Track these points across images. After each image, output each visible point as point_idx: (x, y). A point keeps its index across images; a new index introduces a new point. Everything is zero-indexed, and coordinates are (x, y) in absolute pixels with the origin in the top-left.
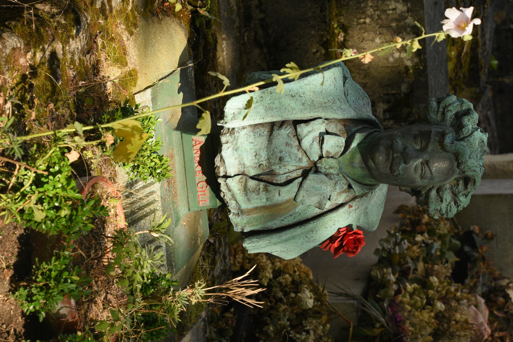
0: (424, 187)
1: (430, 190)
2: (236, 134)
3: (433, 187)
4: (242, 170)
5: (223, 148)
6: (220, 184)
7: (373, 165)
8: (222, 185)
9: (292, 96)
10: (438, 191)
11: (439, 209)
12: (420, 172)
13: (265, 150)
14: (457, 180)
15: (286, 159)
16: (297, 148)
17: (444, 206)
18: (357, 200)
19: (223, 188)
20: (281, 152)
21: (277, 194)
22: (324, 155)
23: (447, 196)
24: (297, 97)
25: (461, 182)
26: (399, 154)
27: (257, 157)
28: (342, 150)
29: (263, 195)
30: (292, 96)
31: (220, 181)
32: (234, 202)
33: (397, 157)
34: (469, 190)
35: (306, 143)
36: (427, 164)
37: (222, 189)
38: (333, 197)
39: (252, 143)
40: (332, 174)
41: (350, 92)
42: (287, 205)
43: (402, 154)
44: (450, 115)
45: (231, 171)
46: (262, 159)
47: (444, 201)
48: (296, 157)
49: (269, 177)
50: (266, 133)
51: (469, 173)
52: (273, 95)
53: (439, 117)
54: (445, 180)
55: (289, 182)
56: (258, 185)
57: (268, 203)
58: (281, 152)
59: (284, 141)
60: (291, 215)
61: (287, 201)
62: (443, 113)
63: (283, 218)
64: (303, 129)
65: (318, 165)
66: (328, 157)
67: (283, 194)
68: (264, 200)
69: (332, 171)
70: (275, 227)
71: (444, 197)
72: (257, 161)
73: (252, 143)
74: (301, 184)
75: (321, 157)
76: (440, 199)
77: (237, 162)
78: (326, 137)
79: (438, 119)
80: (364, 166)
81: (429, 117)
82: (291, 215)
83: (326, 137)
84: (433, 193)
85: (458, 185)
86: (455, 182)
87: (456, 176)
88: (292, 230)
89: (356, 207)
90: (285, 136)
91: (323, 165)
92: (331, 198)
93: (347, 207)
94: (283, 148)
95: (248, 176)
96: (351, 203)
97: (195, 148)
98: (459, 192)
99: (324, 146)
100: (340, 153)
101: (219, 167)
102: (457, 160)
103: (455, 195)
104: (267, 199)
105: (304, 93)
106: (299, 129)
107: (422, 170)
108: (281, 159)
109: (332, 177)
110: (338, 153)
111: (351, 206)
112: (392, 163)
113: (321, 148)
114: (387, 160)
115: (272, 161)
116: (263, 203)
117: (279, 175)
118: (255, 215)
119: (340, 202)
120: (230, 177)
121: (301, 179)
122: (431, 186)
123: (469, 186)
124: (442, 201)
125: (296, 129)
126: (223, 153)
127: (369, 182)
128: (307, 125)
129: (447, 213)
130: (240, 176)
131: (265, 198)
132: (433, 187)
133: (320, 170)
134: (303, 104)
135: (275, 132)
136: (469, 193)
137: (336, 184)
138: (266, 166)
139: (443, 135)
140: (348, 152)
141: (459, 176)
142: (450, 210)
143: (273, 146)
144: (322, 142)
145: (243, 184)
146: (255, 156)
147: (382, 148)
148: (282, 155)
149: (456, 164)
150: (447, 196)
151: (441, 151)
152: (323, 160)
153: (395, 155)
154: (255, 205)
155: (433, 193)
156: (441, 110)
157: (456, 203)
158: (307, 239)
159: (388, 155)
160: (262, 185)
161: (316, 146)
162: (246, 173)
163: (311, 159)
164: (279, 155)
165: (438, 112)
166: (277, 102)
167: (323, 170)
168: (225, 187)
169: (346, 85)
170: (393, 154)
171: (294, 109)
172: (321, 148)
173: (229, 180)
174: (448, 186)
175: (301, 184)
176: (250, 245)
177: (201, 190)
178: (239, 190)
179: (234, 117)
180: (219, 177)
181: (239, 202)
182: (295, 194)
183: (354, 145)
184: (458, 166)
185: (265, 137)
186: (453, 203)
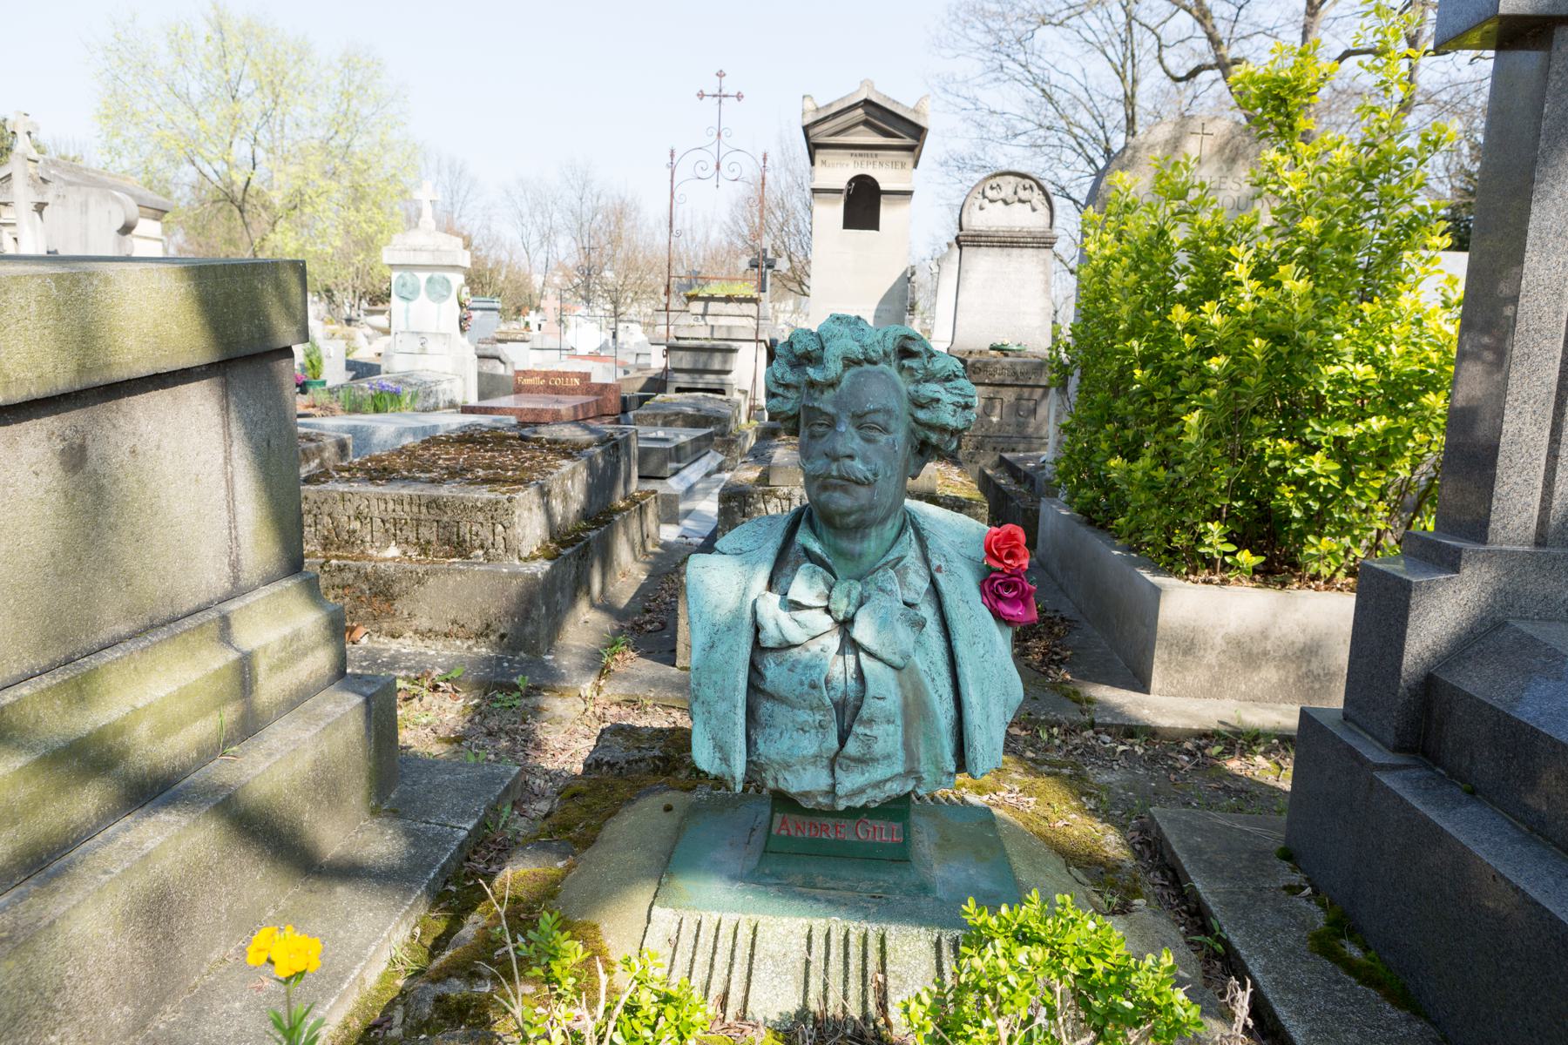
0: (913, 432)
1: (916, 420)
2: (763, 760)
3: (912, 415)
4: (826, 762)
5: (784, 788)
6: (848, 808)
7: (853, 517)
8: (851, 804)
9: (712, 647)
10: (922, 407)
11: (952, 407)
12: (876, 434)
13: (796, 711)
14: (901, 369)
15: (815, 676)
16: (803, 653)
17: (946, 398)
18: (930, 556)
19: (859, 802)
20: (802, 684)
21: (881, 702)
22: (825, 604)
23: (931, 389)
24: (716, 638)
25: (906, 362)
26: (834, 466)
27: (807, 728)
28: (821, 569)
29: (878, 730)
30: (712, 647)
31: (842, 805)
32: (888, 785)
33: (839, 470)
34: (922, 349)
35: (795, 634)
36: (860, 417)
37: (858, 806)
38: (911, 597)
39: (781, 734)
40: (861, 594)
41: (738, 546)
42: (909, 686)
43: (836, 458)
44: (790, 377)
45: (824, 781)
46: (810, 720)
47: (937, 395)
48: (817, 656)
49: (848, 713)
50: (768, 705)
51: (890, 345)
52: (703, 680)
53: (792, 394)
54: (898, 391)
55: (860, 675)
56: (857, 736)
57: (899, 722)
58: (802, 684)
59: (785, 673)
60: (933, 680)
61: (901, 685)
62: (787, 386)
63: (936, 697)
64: (770, 636)
65: (841, 618)
66: (829, 598)
67: (883, 693)
68: (891, 728)
69: (855, 594)
70: (952, 712)
71: (930, 394)
72: (813, 731)
73: (781, 734)
74: (871, 654)
75: (827, 610)
76: (934, 405)
77: (811, 769)
78: (791, 596)
79: (795, 396)
80: (859, 535)
81: (791, 413)
82: (933, 680)
83: (791, 596)
84: (922, 415)
85: (911, 368)
86: (905, 373)
87: (892, 371)
88: (961, 681)
89: (943, 559)
90: (778, 670)
91: (842, 607)
92: (910, 601)
93: (938, 576)
94: (796, 678)
95: (837, 754)
96: (933, 568)
97: (793, 832)
98: (926, 368)
99: (805, 602)
100: (826, 574)
101: (819, 803)
102: (858, 363)
103: (929, 378)
104: (889, 722)
105: (714, 625)
106: (770, 644)
107: (869, 428)
108: (814, 686)
109: (866, 594)
110: (824, 579)
111: (939, 569)
112: (848, 480)
113: (810, 608)
114: (845, 490)
115: (815, 702)
116: (896, 731)
117: (845, 693)
118: (922, 749)
119: (926, 585)
120: (834, 786)
121: (862, 655)
122: (910, 418)
123: (915, 348)
124: (938, 400)
125: (772, 649)
126: (793, 790)
127: (895, 530)
128: (763, 628)
129: (965, 396)
130: (837, 768)
131: (886, 726)
132: (912, 415)
133: (850, 616)
134: (729, 629)
135: (768, 687)
136: (927, 349)
137: (882, 590)
138: (824, 715)
139: (812, 384)
140: (829, 561)
141: (894, 364)
142: (961, 389)
143: (792, 697)
144: (797, 606)
145: (852, 764)
146: (805, 732)
147: (824, 497)
148: (806, 682)
149: (867, 366)
150: (931, 389)
151: (838, 390)
152: (832, 607)
153: (835, 473)
154: (899, 746)
155: (922, 415)
156: (780, 391)
157: (948, 379)
158: (987, 656)
159: (835, 487)
160: (858, 729)
161: (802, 615)
162: (832, 754)
163: (829, 628)
164: (806, 687)
165: (785, 397)
166: (714, 677)
167: (852, 609)
168: (856, 799)
169: (725, 550)
170: (833, 477)
171: (731, 648)
172: (810, 608)
173: (840, 791)
174: (912, 388)
175: (871, 654)
176: (980, 765)
177: (871, 835)
178: (863, 774)
179: (725, 760)
180: (833, 806)
181: (889, 775)
182: (889, 669)
183: (816, 547)
184: (874, 363)
185: (776, 708)
186: (948, 385)
